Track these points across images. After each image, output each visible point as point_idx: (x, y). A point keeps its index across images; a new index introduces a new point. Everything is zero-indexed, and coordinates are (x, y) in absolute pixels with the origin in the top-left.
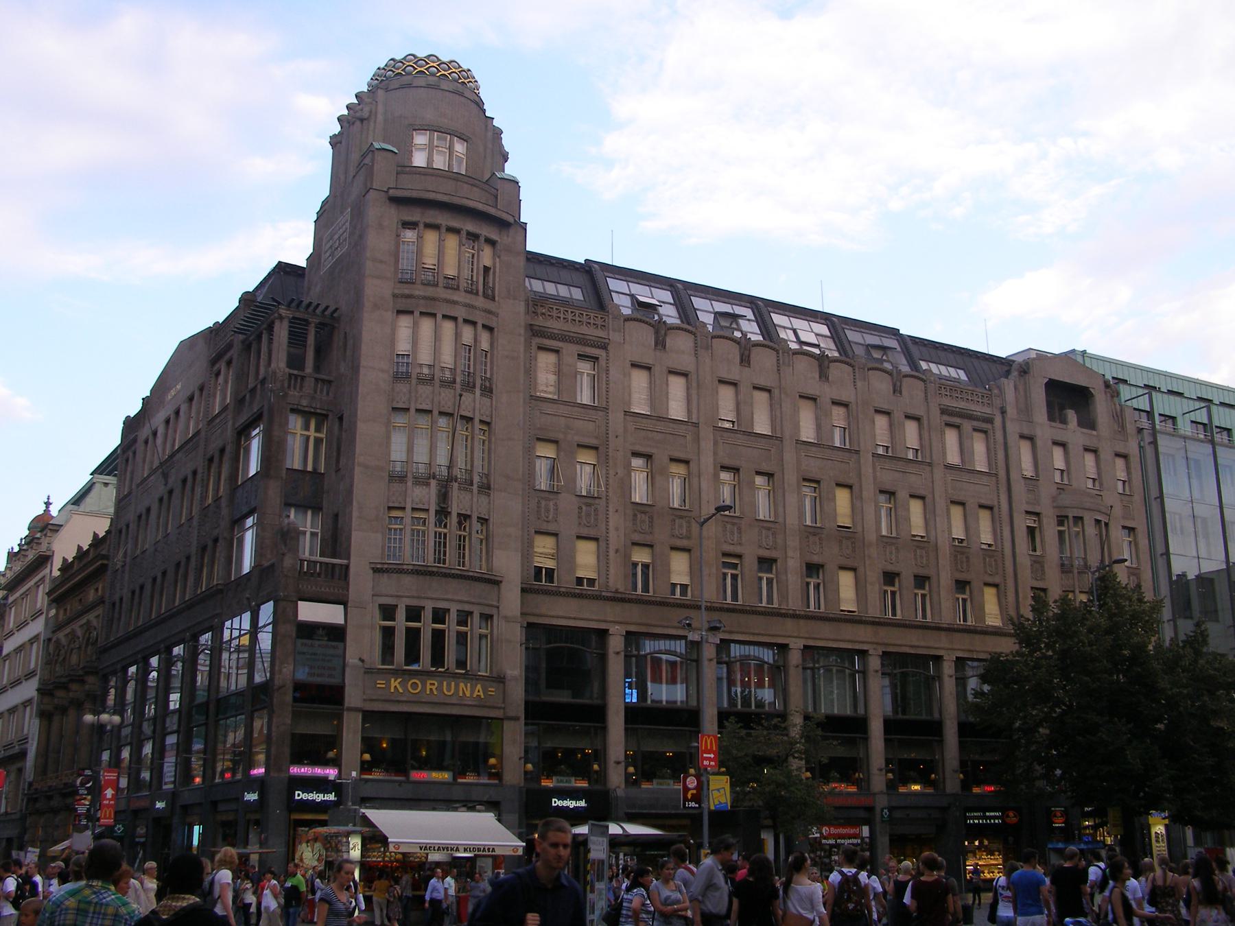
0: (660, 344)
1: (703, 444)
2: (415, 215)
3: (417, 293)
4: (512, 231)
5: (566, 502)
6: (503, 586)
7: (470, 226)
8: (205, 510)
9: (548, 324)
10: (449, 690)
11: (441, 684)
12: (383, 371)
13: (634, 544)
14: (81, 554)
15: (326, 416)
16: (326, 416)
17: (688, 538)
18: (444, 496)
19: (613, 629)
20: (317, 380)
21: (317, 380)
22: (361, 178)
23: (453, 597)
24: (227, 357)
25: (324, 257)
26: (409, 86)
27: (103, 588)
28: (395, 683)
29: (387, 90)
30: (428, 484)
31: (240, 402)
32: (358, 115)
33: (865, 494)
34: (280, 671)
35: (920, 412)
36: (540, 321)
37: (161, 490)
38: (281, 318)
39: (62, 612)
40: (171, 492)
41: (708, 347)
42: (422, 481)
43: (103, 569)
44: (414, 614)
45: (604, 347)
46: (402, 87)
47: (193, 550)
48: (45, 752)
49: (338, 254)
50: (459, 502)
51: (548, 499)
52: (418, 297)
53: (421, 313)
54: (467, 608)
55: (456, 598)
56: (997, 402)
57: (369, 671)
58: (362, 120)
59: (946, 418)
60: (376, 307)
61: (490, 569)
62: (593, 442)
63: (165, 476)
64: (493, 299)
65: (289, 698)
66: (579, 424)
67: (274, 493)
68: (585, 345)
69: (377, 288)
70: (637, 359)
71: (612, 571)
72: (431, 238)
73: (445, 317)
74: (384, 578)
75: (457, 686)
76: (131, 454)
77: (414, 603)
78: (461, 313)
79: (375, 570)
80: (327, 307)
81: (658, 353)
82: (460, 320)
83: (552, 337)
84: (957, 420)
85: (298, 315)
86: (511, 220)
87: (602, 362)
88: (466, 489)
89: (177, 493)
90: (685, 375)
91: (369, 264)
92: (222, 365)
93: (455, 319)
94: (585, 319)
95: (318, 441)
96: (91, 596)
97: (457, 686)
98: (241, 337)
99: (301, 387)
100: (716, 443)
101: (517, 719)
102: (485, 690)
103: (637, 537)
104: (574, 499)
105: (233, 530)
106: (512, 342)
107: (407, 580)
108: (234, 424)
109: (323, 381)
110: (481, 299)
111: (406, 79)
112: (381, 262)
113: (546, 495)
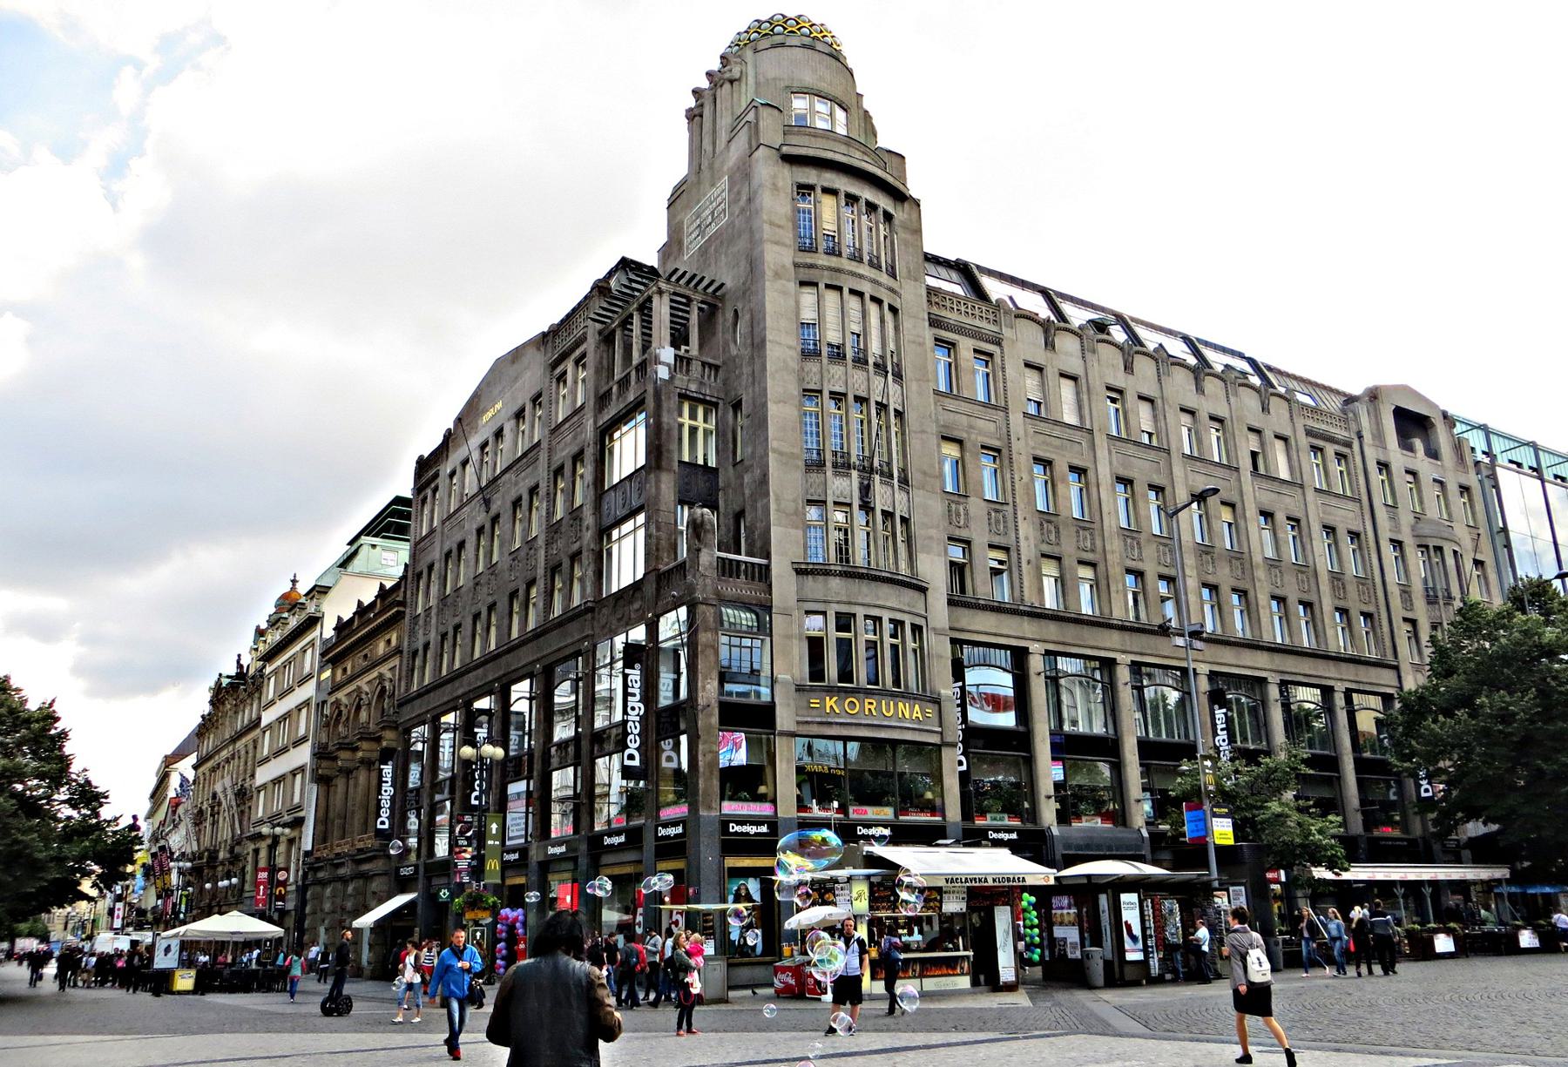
0: (1050, 345)
2: (810, 176)
3: (820, 262)
4: (906, 205)
5: (976, 507)
6: (929, 593)
7: (867, 193)
8: (553, 529)
9: (943, 313)
11: (879, 704)
12: (790, 347)
13: (1043, 555)
14: (362, 610)
15: (716, 405)
17: (1093, 551)
18: (865, 490)
19: (1035, 647)
20: (704, 364)
21: (704, 364)
22: (742, 139)
23: (891, 601)
24: (578, 353)
26: (782, 45)
27: (399, 638)
28: (830, 702)
29: (756, 51)
30: (849, 476)
31: (602, 400)
35: (1287, 432)
36: (935, 310)
37: (481, 518)
38: (660, 292)
39: (339, 672)
40: (495, 520)
41: (1094, 351)
42: (843, 467)
43: (399, 616)
44: (844, 622)
45: (998, 343)
46: (774, 46)
47: (540, 571)
48: (323, 821)
49: (714, 228)
50: (882, 496)
51: (958, 503)
52: (823, 268)
54: (899, 616)
55: (889, 604)
56: (1353, 426)
57: (800, 689)
58: (732, 82)
59: (1311, 440)
60: (777, 275)
61: (914, 575)
62: (996, 443)
63: (487, 503)
64: (894, 276)
65: (715, 720)
66: (980, 423)
67: (667, 486)
68: (981, 339)
69: (778, 255)
70: (1030, 359)
71: (1026, 584)
72: (828, 203)
73: (852, 292)
74: (809, 581)
75: (896, 705)
76: (429, 492)
77: (844, 609)
78: (867, 288)
79: (799, 572)
80: (712, 282)
81: (1049, 354)
82: (867, 297)
83: (948, 328)
84: (1320, 443)
85: (678, 290)
87: (998, 359)
88: (887, 484)
89: (505, 519)
90: (1074, 379)
91: (766, 227)
92: (569, 365)
93: (860, 294)
94: (977, 312)
95: (707, 433)
96: (381, 648)
97: (896, 705)
98: (598, 326)
99: (688, 371)
100: (1110, 452)
101: (954, 745)
102: (923, 711)
103: (1046, 548)
104: (984, 504)
105: (601, 540)
106: (917, 329)
107: (835, 583)
108: (595, 422)
109: (710, 366)
113: (956, 498)
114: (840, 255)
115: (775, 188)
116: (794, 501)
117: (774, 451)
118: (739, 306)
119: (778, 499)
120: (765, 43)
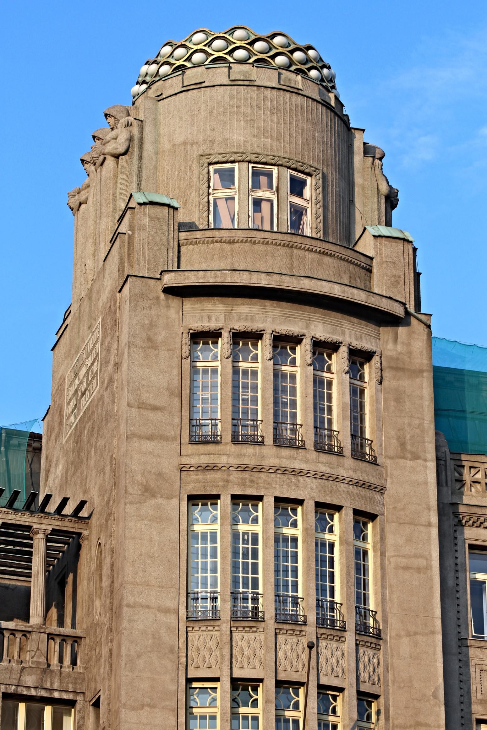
3: (223, 460)
12: (166, 611)
16: (72, 703)
25: (66, 413)
26: (199, 85)
32: (109, 148)
49: (86, 402)
52: (228, 468)
53: (234, 498)
58: (117, 157)
60: (149, 492)
64: (374, 462)
80: (65, 501)
86: (399, 311)
110: (349, 462)
111: (192, 76)
112: (155, 408)
114: (262, 443)
115: (151, 343)
118: (102, 541)
120: (175, 84)
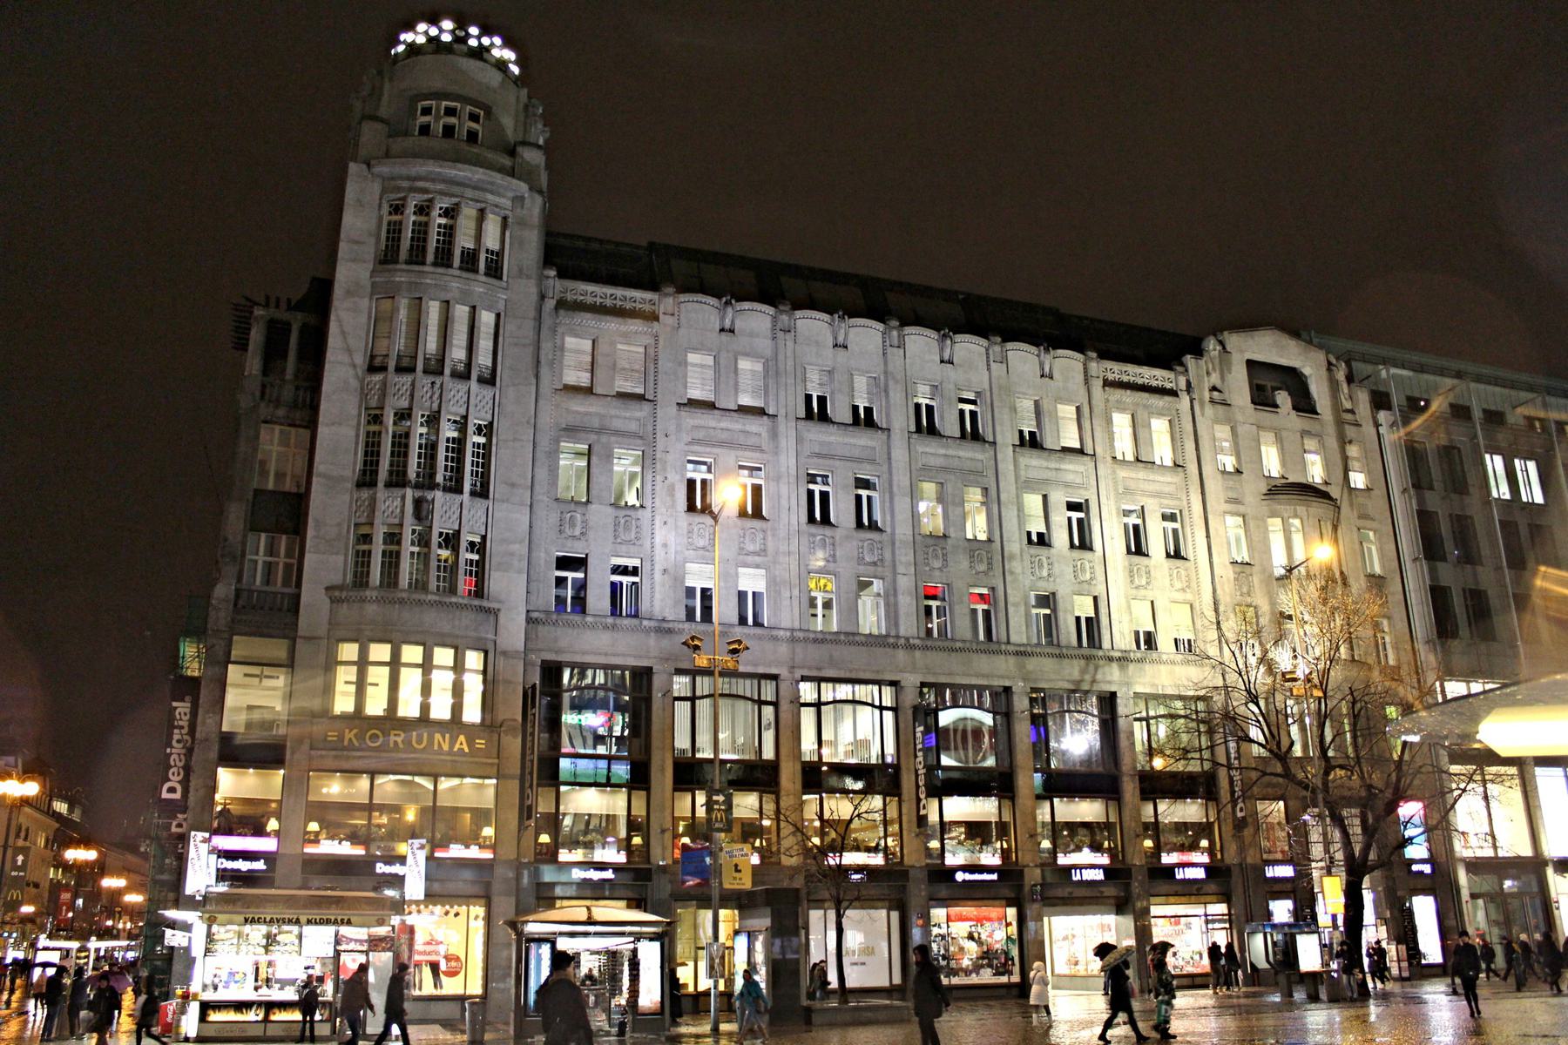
1: (783, 442)
6: (502, 617)
10: (419, 742)
33: (1003, 497)
34: (204, 723)
60: (349, 293)
75: (431, 739)
102: (470, 743)
116: (339, 525)
117: (319, 475)
119: (318, 523)
